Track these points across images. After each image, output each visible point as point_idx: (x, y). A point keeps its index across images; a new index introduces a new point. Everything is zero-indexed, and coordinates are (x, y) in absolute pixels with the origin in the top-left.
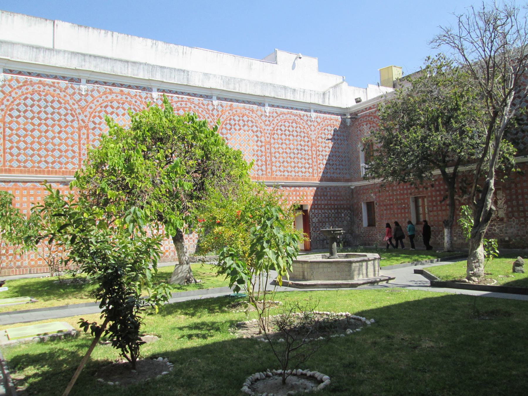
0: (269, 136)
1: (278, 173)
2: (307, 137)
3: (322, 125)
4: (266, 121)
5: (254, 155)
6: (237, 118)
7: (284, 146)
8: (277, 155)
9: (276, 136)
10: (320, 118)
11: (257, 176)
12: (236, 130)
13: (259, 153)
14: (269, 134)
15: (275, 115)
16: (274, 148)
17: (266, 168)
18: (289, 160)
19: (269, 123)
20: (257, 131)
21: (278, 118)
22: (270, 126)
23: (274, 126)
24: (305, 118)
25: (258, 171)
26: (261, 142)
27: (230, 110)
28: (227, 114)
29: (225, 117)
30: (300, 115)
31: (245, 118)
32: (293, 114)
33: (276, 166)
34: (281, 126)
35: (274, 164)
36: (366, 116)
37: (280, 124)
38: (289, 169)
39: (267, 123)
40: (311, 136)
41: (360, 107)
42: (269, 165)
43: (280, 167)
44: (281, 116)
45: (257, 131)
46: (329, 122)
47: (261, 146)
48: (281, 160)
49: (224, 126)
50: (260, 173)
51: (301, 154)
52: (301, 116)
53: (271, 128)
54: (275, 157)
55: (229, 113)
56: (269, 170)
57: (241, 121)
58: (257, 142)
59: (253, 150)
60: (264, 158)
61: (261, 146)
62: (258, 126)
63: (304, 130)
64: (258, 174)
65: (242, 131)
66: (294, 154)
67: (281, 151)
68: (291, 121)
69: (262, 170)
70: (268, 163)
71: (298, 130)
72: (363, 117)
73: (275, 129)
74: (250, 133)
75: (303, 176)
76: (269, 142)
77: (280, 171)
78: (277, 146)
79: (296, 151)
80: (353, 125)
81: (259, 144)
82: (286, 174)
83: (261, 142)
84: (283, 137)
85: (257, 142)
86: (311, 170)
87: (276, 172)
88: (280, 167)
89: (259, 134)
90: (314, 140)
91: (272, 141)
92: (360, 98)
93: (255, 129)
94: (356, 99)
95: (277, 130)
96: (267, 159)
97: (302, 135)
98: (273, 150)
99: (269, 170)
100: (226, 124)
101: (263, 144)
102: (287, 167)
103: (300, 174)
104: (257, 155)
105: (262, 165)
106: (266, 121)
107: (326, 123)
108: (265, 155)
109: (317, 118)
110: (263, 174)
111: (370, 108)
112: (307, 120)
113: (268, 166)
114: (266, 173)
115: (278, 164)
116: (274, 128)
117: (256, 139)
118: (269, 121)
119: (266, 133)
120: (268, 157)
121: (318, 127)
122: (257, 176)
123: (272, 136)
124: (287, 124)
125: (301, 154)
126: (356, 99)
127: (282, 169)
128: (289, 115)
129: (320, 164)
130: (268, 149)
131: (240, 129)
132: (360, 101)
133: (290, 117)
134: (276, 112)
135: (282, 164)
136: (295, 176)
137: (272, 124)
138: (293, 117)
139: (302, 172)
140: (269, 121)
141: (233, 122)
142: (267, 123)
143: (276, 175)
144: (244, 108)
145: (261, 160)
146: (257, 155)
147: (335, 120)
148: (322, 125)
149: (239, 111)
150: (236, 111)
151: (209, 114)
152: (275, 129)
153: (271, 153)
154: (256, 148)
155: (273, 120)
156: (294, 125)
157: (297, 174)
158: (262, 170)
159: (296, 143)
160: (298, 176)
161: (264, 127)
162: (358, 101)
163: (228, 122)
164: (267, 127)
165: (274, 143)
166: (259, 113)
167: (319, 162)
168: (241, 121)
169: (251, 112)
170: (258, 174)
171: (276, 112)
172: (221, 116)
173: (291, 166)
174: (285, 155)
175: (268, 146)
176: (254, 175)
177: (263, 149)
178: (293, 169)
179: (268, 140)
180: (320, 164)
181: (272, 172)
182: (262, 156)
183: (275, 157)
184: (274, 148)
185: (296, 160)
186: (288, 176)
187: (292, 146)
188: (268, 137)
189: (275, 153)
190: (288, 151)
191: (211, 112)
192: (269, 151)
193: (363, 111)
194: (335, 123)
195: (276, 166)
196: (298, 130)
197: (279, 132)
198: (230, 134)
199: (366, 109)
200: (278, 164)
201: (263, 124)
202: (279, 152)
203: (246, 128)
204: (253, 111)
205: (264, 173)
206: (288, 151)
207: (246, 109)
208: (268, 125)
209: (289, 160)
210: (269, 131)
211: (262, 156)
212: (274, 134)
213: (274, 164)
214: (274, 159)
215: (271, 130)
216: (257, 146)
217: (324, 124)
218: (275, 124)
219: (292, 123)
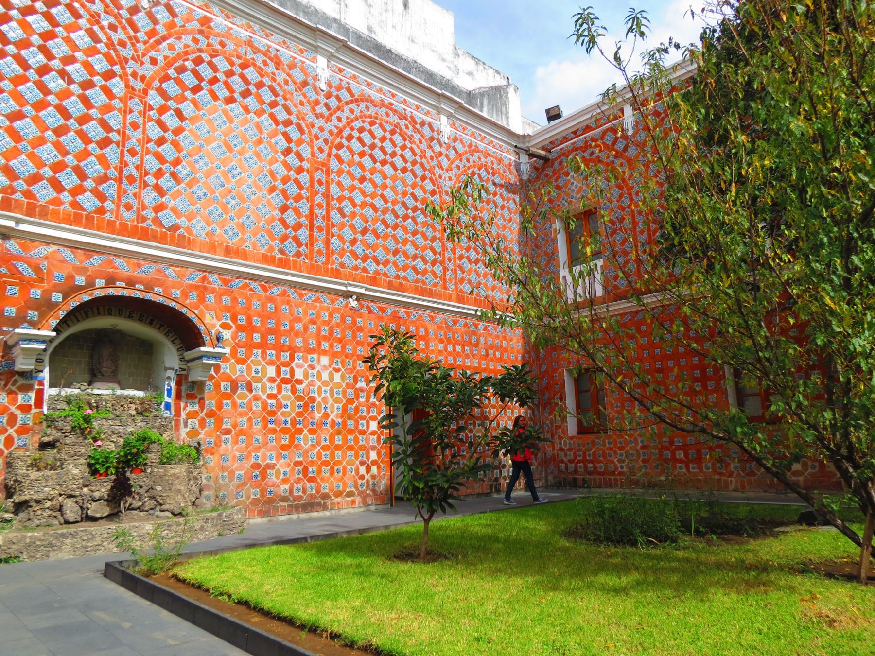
0: (326, 148)
1: (349, 261)
2: (431, 179)
3: (468, 160)
4: (317, 103)
5: (272, 189)
6: (222, 64)
7: (368, 187)
8: (348, 208)
9: (344, 154)
10: (461, 141)
11: (279, 256)
12: (215, 97)
13: (292, 189)
14: (326, 141)
15: (345, 95)
16: (339, 184)
17: (311, 236)
18: (380, 227)
19: (326, 113)
20: (287, 123)
21: (353, 106)
22: (328, 120)
23: (340, 125)
24: (426, 130)
25: (284, 239)
26: (299, 156)
27: (201, 32)
28: (187, 39)
29: (179, 46)
30: (412, 117)
31: (251, 74)
32: (395, 111)
33: (341, 238)
34: (361, 130)
35: (334, 230)
36: (577, 149)
37: (357, 124)
38: (380, 254)
39: (321, 109)
40: (441, 181)
41: (559, 127)
42: (320, 229)
43: (353, 242)
44: (363, 105)
45: (287, 123)
46: (483, 160)
47: (300, 170)
48: (358, 223)
49: (171, 72)
50: (290, 247)
51: (414, 219)
52: (415, 122)
53: (330, 126)
54: (340, 211)
55: (195, 40)
56: (319, 245)
57: (236, 79)
58: (287, 152)
59: (272, 173)
60: (304, 207)
61: (300, 170)
62: (293, 108)
63: (424, 160)
64: (282, 251)
65: (235, 109)
66: (396, 216)
67: (359, 199)
68: (388, 127)
69: (298, 243)
70: (316, 224)
71: (408, 154)
72: (565, 154)
73: (346, 133)
74: (265, 121)
75: (417, 281)
76: (323, 164)
77: (355, 255)
78: (347, 182)
79: (401, 212)
80: (538, 178)
81: (292, 159)
82: (372, 267)
83: (299, 156)
84: (367, 161)
85: (287, 152)
86: (438, 269)
87: (341, 256)
88: (353, 242)
89: (295, 134)
90: (447, 192)
91: (334, 165)
92: (558, 107)
93: (282, 116)
94: (548, 111)
95: (350, 138)
96: (317, 211)
97: (419, 172)
98: (334, 190)
99: (319, 245)
100: (181, 70)
101: (306, 165)
102: (374, 248)
103: (411, 275)
104: (284, 192)
105: (298, 226)
106: (317, 103)
107: (475, 158)
108: (310, 199)
109: (455, 140)
110: (298, 254)
111: (588, 128)
112: (432, 139)
113: (316, 233)
114: (312, 251)
115: (348, 234)
116: (341, 131)
117: (284, 144)
118: (327, 106)
119: (317, 138)
120: (320, 206)
121: (457, 162)
122: (279, 256)
123: (334, 151)
124: (378, 131)
125: (414, 219)
126: (548, 111)
127: (359, 249)
128: (384, 110)
129: (461, 257)
130: (320, 183)
131: (230, 100)
132: (558, 116)
133: (388, 115)
134: (349, 90)
135: (359, 236)
136: (398, 277)
137: (334, 118)
138: (394, 118)
139: (414, 268)
140: (327, 106)
141: (206, 72)
142: (321, 109)
143: (342, 265)
144: (249, 43)
145: (297, 211)
146: (284, 192)
147: (496, 159)
148: (468, 160)
149: (230, 47)
150: (222, 44)
151: (117, 17)
152: (346, 133)
153: (327, 196)
154: (281, 171)
155: (338, 108)
156: (397, 138)
157: (402, 273)
158: (298, 243)
159: (400, 188)
160: (405, 278)
161: (311, 118)
162: (553, 115)
163: (189, 64)
164: (320, 122)
165: (340, 172)
166: (298, 76)
167: (458, 252)
168: (236, 79)
169: (271, 67)
170: (282, 251)
171: (349, 90)
172: (164, 38)
173: (386, 249)
174: (369, 212)
175: (318, 175)
176: (271, 249)
177: (304, 178)
178: (390, 257)
179: (322, 157)
180: (461, 257)
181: (330, 253)
182: (298, 198)
183: (340, 211)
184: (339, 184)
185: (400, 233)
186: (377, 272)
187: (389, 193)
188: (321, 150)
189: (340, 199)
190: (378, 202)
191: (124, 13)
192: (322, 189)
193: (566, 139)
194: (496, 166)
195: (341, 238)
196: (408, 154)
197: (355, 145)
198: (195, 103)
199: (575, 133)
200: (348, 234)
201: (307, 109)
202: (351, 200)
203: (251, 101)
204: (278, 64)
205: (303, 249)
206: (378, 202)
207: (256, 51)
208: (322, 115)
209: (380, 227)
210: (326, 135)
211: (298, 198)
212: (340, 146)
213: (334, 230)
214: (336, 217)
215: (331, 133)
216: (286, 165)
217: (471, 159)
218: (344, 121)
219: (393, 132)
